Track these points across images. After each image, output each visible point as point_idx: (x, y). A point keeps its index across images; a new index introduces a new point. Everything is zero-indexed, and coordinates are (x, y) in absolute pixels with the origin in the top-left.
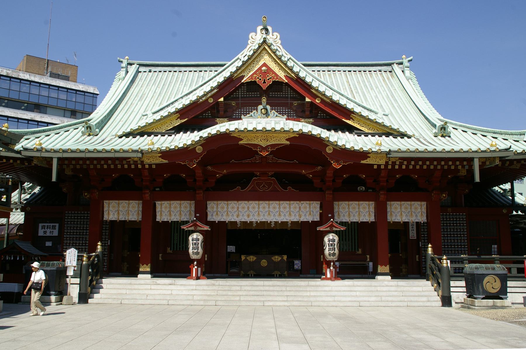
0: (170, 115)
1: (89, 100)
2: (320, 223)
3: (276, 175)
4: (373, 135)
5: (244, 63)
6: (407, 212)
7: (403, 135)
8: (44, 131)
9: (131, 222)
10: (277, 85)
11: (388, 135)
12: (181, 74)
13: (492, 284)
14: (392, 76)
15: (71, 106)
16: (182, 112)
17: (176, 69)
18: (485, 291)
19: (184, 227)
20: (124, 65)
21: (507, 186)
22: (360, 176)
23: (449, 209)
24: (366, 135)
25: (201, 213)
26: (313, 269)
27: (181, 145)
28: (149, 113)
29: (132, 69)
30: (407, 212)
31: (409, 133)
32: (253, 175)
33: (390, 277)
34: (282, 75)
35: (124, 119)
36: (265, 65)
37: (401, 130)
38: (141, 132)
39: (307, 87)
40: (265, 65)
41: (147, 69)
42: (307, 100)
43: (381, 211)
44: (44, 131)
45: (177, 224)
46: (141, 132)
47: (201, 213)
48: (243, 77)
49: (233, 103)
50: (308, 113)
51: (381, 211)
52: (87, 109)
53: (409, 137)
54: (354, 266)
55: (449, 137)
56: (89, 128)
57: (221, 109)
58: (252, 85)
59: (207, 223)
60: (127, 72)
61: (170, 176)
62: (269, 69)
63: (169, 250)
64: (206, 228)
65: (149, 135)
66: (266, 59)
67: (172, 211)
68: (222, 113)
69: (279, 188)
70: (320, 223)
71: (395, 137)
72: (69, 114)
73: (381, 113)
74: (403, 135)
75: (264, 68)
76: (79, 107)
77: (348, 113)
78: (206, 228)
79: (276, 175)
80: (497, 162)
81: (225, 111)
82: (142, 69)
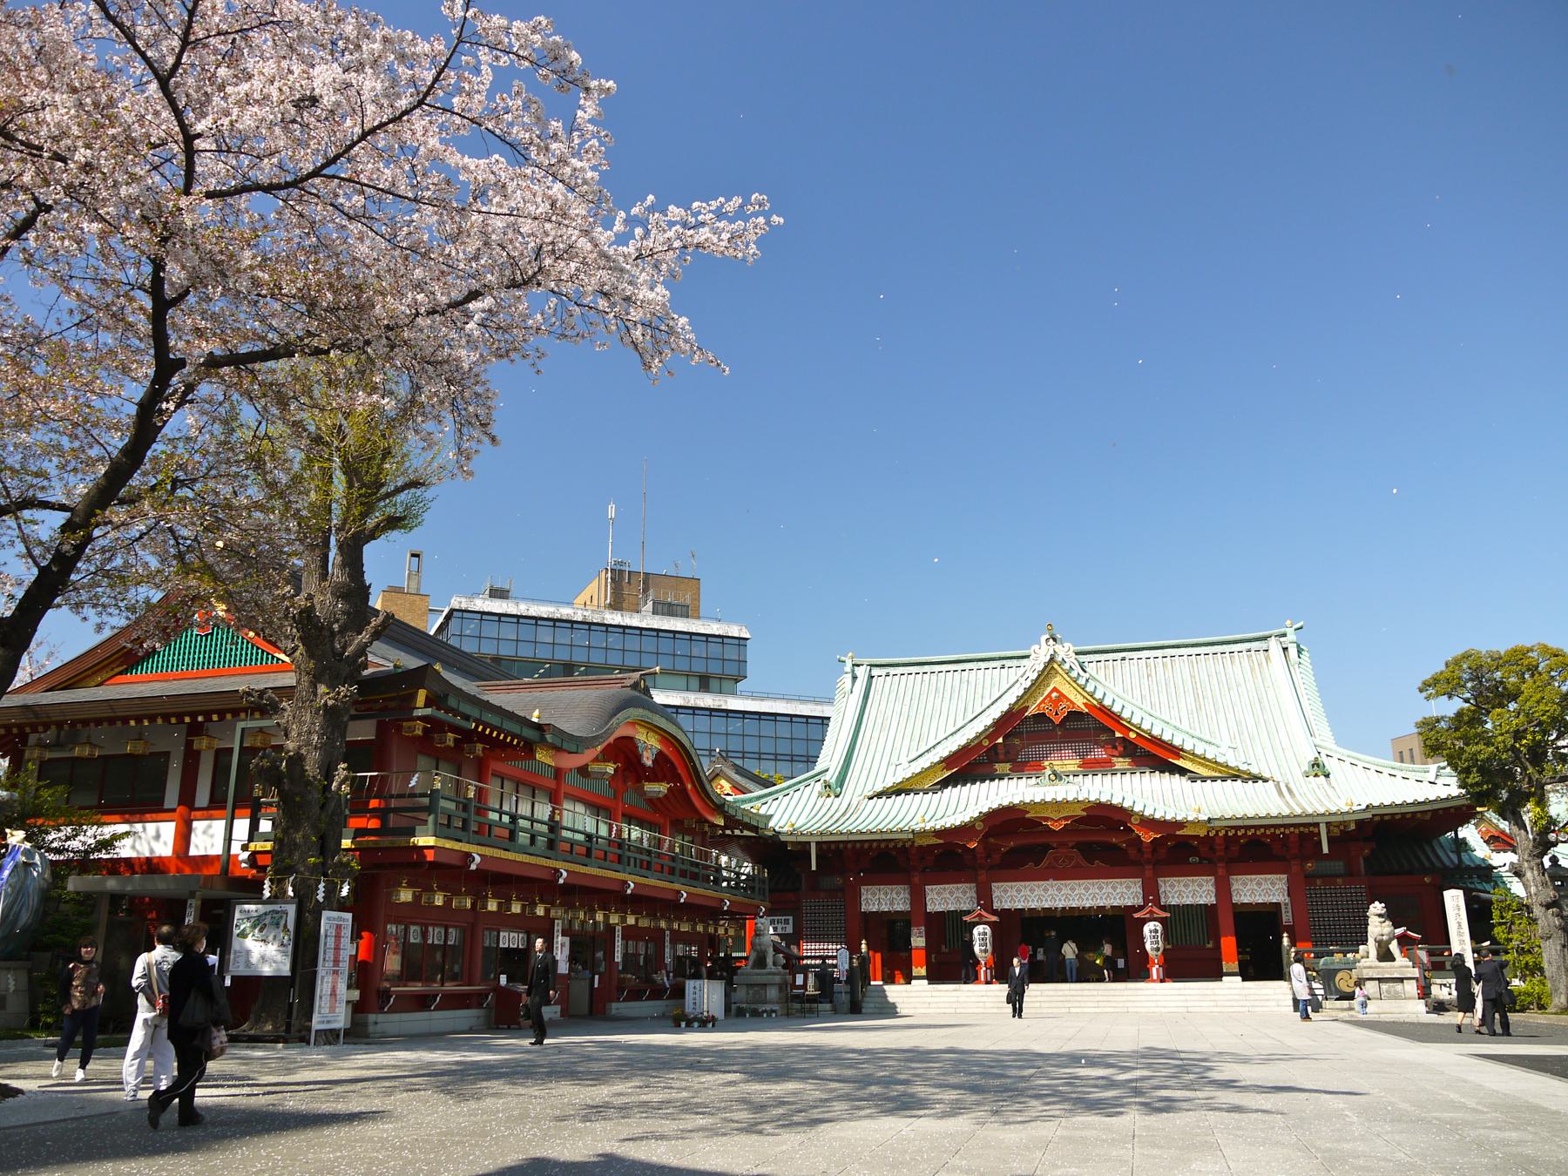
0: (933, 766)
1: (731, 653)
2: (1140, 908)
3: (1079, 846)
4: (1214, 779)
5: (1027, 690)
6: (1259, 889)
7: (1256, 778)
8: (770, 794)
9: (897, 912)
10: (1075, 715)
11: (1235, 777)
12: (934, 677)
13: (1343, 982)
14: (1267, 659)
15: (699, 667)
16: (948, 761)
17: (927, 668)
18: (1338, 991)
19: (967, 918)
20: (848, 668)
21: (1451, 834)
22: (1179, 848)
23: (1339, 880)
24: (1204, 779)
25: (985, 897)
26: (1133, 969)
27: (958, 823)
28: (904, 760)
29: (862, 672)
30: (1259, 889)
31: (1266, 775)
32: (1047, 847)
33: (1239, 978)
34: (1079, 702)
35: (867, 765)
36: (1055, 689)
37: (1255, 771)
38: (898, 791)
39: (1116, 718)
40: (1055, 689)
41: (883, 671)
42: (1118, 735)
43: (1223, 889)
44: (770, 794)
45: (957, 915)
46: (898, 791)
47: (985, 897)
48: (1027, 708)
49: (1017, 742)
50: (1121, 749)
51: (1223, 889)
52: (731, 669)
53: (1266, 781)
54: (1191, 961)
55: (1327, 776)
56: (827, 786)
57: (1001, 751)
58: (1040, 717)
59: (994, 912)
60: (855, 678)
61: (944, 854)
62: (1062, 695)
63: (944, 949)
64: (994, 918)
65: (907, 792)
66: (1056, 682)
67: (945, 898)
68: (1002, 757)
69: (1084, 863)
70: (1140, 908)
71: (1245, 781)
72: (695, 682)
73: (1225, 743)
74: (1256, 778)
75: (1054, 695)
76: (714, 668)
77: (1177, 751)
78: (994, 918)
79: (1079, 846)
80: (1353, 827)
81: (1007, 752)
82: (876, 672)
